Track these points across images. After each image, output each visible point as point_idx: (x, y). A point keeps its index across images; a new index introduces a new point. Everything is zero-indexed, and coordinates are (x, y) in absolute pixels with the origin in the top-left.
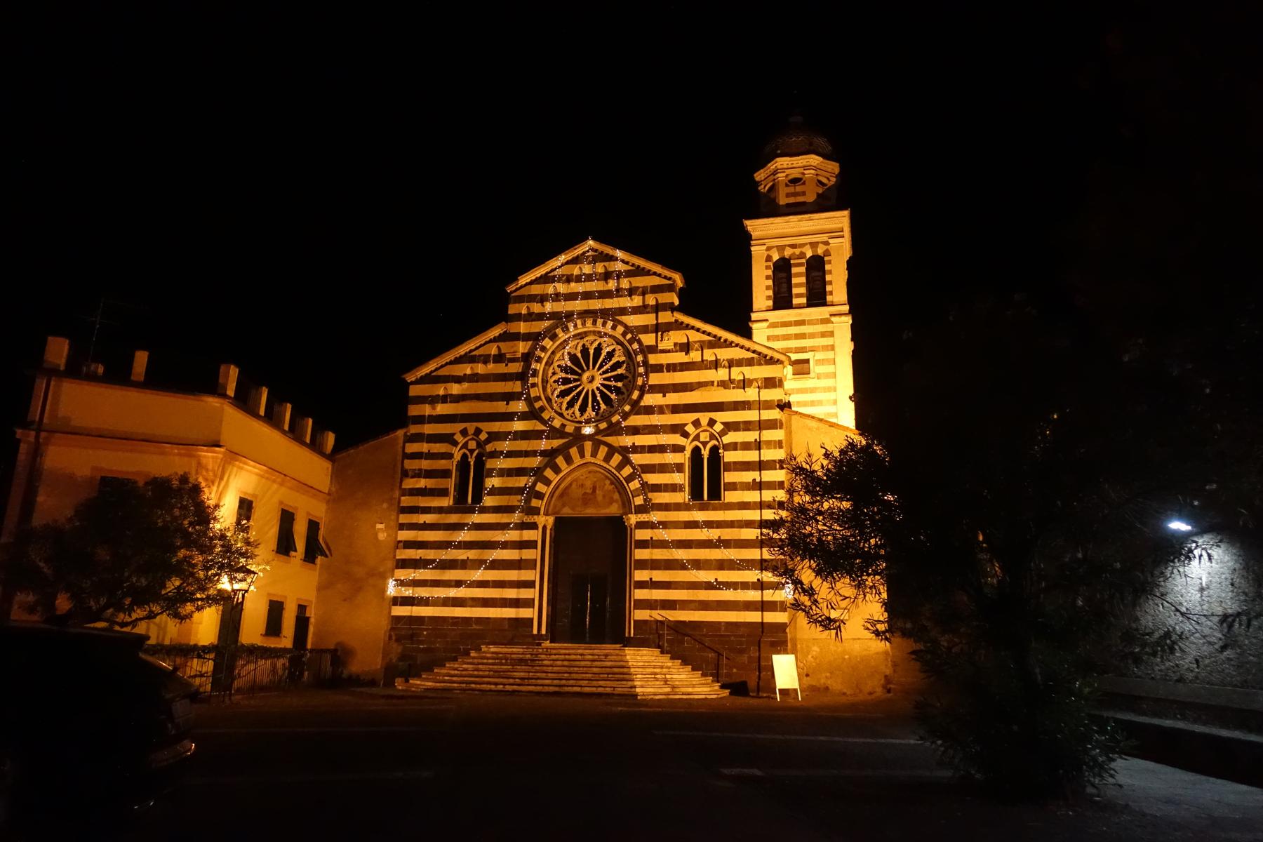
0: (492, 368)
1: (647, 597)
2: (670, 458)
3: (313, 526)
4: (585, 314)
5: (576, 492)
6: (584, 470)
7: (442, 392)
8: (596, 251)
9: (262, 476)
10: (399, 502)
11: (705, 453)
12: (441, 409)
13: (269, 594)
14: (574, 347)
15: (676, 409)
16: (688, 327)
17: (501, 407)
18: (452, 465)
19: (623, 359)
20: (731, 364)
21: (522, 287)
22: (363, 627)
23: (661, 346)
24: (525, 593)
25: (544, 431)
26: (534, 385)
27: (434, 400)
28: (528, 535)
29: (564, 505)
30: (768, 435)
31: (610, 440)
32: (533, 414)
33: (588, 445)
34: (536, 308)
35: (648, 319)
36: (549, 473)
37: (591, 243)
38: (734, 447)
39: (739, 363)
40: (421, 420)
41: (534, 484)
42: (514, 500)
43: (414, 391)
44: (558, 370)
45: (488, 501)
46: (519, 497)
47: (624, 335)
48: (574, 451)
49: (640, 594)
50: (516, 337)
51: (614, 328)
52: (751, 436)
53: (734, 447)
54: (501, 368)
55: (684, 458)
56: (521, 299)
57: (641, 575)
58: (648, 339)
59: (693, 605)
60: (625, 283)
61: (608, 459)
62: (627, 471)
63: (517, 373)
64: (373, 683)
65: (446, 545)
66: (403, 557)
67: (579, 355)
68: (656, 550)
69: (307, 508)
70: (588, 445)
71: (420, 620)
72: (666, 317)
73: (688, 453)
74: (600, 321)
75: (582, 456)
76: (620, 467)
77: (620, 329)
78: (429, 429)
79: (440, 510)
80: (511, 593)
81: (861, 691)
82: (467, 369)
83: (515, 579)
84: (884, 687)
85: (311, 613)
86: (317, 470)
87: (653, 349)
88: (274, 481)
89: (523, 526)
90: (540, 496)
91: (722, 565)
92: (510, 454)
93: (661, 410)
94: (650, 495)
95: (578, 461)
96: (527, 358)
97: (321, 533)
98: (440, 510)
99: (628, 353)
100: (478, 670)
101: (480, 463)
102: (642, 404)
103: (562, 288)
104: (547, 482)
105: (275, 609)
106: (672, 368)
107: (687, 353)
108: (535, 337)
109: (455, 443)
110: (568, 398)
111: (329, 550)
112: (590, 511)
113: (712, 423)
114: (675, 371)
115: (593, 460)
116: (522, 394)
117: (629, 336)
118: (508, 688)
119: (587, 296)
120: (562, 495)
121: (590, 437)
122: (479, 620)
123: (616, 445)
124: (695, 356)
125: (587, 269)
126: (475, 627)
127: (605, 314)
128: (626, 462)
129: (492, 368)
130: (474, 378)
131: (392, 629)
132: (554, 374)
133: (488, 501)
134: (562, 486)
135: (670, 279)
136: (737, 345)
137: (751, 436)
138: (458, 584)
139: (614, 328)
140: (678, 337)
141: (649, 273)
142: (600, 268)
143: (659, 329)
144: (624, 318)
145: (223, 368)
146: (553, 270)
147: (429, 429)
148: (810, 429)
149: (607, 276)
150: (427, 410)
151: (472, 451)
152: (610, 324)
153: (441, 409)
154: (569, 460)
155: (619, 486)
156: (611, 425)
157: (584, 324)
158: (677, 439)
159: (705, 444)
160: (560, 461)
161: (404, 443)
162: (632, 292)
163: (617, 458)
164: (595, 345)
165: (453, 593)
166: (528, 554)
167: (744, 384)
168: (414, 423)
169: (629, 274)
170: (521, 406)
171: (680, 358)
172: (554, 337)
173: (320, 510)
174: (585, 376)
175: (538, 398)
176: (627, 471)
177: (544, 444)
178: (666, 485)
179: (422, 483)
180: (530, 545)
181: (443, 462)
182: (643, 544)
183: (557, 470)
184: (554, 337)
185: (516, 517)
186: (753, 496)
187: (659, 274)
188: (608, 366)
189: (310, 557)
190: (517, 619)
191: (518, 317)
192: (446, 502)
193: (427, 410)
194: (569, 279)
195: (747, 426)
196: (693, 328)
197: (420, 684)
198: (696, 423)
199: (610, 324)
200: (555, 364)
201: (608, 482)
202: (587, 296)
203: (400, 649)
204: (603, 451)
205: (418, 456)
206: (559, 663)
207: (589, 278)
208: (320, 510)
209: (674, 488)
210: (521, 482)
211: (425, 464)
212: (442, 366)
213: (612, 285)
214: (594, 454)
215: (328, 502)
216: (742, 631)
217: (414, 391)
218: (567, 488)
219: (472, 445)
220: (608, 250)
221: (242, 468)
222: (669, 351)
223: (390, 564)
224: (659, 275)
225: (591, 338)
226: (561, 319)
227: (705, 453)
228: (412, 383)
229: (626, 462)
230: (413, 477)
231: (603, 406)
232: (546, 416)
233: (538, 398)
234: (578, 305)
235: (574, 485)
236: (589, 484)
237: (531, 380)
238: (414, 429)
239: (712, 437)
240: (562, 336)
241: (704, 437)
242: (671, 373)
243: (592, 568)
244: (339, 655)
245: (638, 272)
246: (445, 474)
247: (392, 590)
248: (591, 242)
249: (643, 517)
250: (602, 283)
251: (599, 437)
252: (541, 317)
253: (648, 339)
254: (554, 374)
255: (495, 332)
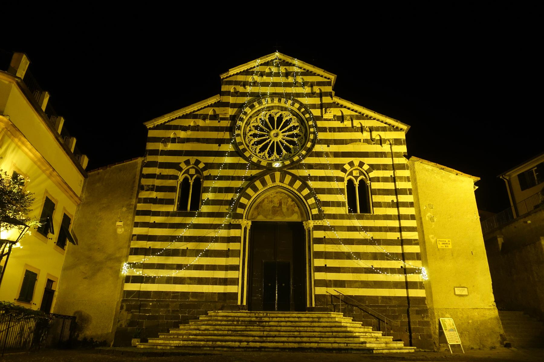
0: (208, 123)
1: (321, 279)
2: (335, 185)
3: (66, 220)
4: (273, 95)
5: (267, 206)
6: (273, 191)
7: (172, 136)
8: (280, 60)
9: (35, 163)
10: (136, 207)
11: (357, 183)
12: (170, 147)
13: (26, 265)
14: (264, 116)
15: (336, 155)
16: (342, 106)
17: (215, 147)
18: (177, 184)
19: (297, 124)
20: (371, 130)
21: (230, 76)
22: (99, 300)
23: (325, 116)
24: (232, 274)
25: (246, 164)
26: (238, 135)
27: (165, 140)
28: (234, 233)
29: (258, 214)
30: (399, 173)
31: (293, 171)
32: (238, 153)
33: (278, 175)
34: (241, 89)
35: (316, 101)
36: (249, 191)
37: (277, 54)
38: (377, 179)
39: (377, 129)
40: (155, 152)
41: (239, 198)
42: (224, 209)
43: (151, 134)
44: (253, 128)
45: (204, 209)
46: (227, 207)
47: (299, 109)
48: (267, 178)
49: (319, 276)
50: (227, 105)
51: (293, 105)
52: (388, 174)
53: (377, 179)
54: (215, 123)
55: (343, 185)
56: (230, 83)
57: (318, 262)
58: (316, 112)
59: (357, 284)
60: (299, 79)
61: (292, 183)
62: (306, 192)
63: (227, 127)
64: (104, 343)
65: (172, 239)
66: (136, 246)
67: (267, 120)
68: (328, 246)
69: (65, 205)
70: (278, 175)
71: (147, 294)
72: (327, 100)
73: (346, 182)
74: (283, 100)
75: (274, 180)
76: (300, 189)
77: (297, 105)
78: (161, 159)
79: (167, 214)
80: (221, 274)
81: (484, 346)
82: (191, 122)
83: (224, 264)
84: (501, 343)
85: (56, 287)
86: (75, 179)
87: (320, 118)
88: (44, 171)
89: (230, 226)
90: (243, 206)
91: (375, 256)
92: (221, 178)
93: (327, 155)
94: (322, 208)
95: (270, 184)
96: (234, 118)
97: (71, 227)
98: (167, 214)
99: (301, 121)
100: (218, 330)
101: (198, 183)
102: (314, 150)
103: (258, 79)
104: (248, 197)
105: (30, 279)
106: (333, 130)
107: (342, 121)
108: (241, 106)
109: (180, 169)
110: (261, 146)
111: (77, 240)
112: (278, 219)
113: (361, 164)
114: (334, 131)
115: (281, 184)
116: (232, 139)
117: (303, 110)
118: (251, 344)
119: (275, 85)
120: (257, 207)
121: (279, 169)
122: (195, 294)
123: (298, 175)
124: (347, 124)
125: (274, 70)
126: (191, 299)
127: (288, 96)
128: (305, 185)
129: (208, 123)
130: (196, 128)
131: (123, 301)
132: (250, 130)
133: (204, 209)
134: (258, 201)
135: (329, 79)
136: (374, 119)
137: (388, 174)
138: (179, 267)
139: (293, 105)
140: (336, 112)
141: (314, 74)
142: (282, 69)
143: (321, 106)
144: (299, 99)
145: (15, 55)
146: (251, 68)
147: (161, 159)
148: (427, 170)
149: (287, 74)
150: (161, 147)
151: (192, 176)
152: (290, 102)
153: (170, 147)
154: (264, 183)
155: (299, 202)
156: (293, 162)
157: (272, 101)
158: (338, 173)
159: (356, 178)
160: (258, 183)
161: (142, 167)
162: (304, 84)
163: (298, 184)
164: (278, 115)
165: (174, 273)
166: (234, 246)
167: (381, 142)
168: (150, 154)
169: (303, 74)
170: (230, 148)
171: (337, 124)
172: (252, 107)
173: (72, 211)
174: (273, 133)
175: (241, 144)
176: (306, 192)
177: (247, 173)
178: (333, 202)
179: (154, 195)
180: (235, 239)
181: (171, 181)
182: (319, 241)
183: (255, 189)
184: (252, 107)
185: (225, 221)
186: (393, 211)
187: (322, 75)
188: (286, 129)
189: (61, 243)
190: (225, 294)
191: (228, 93)
192: (172, 208)
193: (161, 147)
194: (262, 74)
195: (385, 167)
196: (345, 107)
197: (160, 342)
198: (351, 164)
199: (290, 102)
200: (251, 125)
201: (290, 200)
202: (275, 85)
203: (129, 316)
204: (288, 178)
205: (153, 176)
206: (283, 324)
207: (277, 75)
208: (72, 211)
209: (339, 204)
210: (229, 196)
211: (158, 182)
212: (173, 120)
213: (291, 80)
214: (282, 181)
215: (78, 205)
216: (394, 303)
217: (151, 134)
218: (260, 203)
219: (192, 171)
220: (289, 59)
221: (19, 147)
222: (330, 120)
223: (125, 251)
224: (322, 76)
225: (275, 111)
226: (258, 97)
227: (357, 183)
228: (150, 129)
229: (305, 185)
230: (147, 190)
231: (284, 152)
232: (247, 154)
233: (241, 144)
234: (269, 90)
235: (266, 200)
236: (276, 200)
237: (237, 132)
238: (150, 158)
239: (361, 173)
240: (257, 107)
241: (355, 173)
242: (332, 133)
243: (280, 259)
244: (77, 321)
245: (307, 73)
246: (172, 189)
247: (125, 270)
248: (277, 54)
249: (319, 223)
250: (284, 78)
251: (285, 169)
252: (244, 95)
253: (316, 112)
254: (250, 130)
255: (213, 100)
